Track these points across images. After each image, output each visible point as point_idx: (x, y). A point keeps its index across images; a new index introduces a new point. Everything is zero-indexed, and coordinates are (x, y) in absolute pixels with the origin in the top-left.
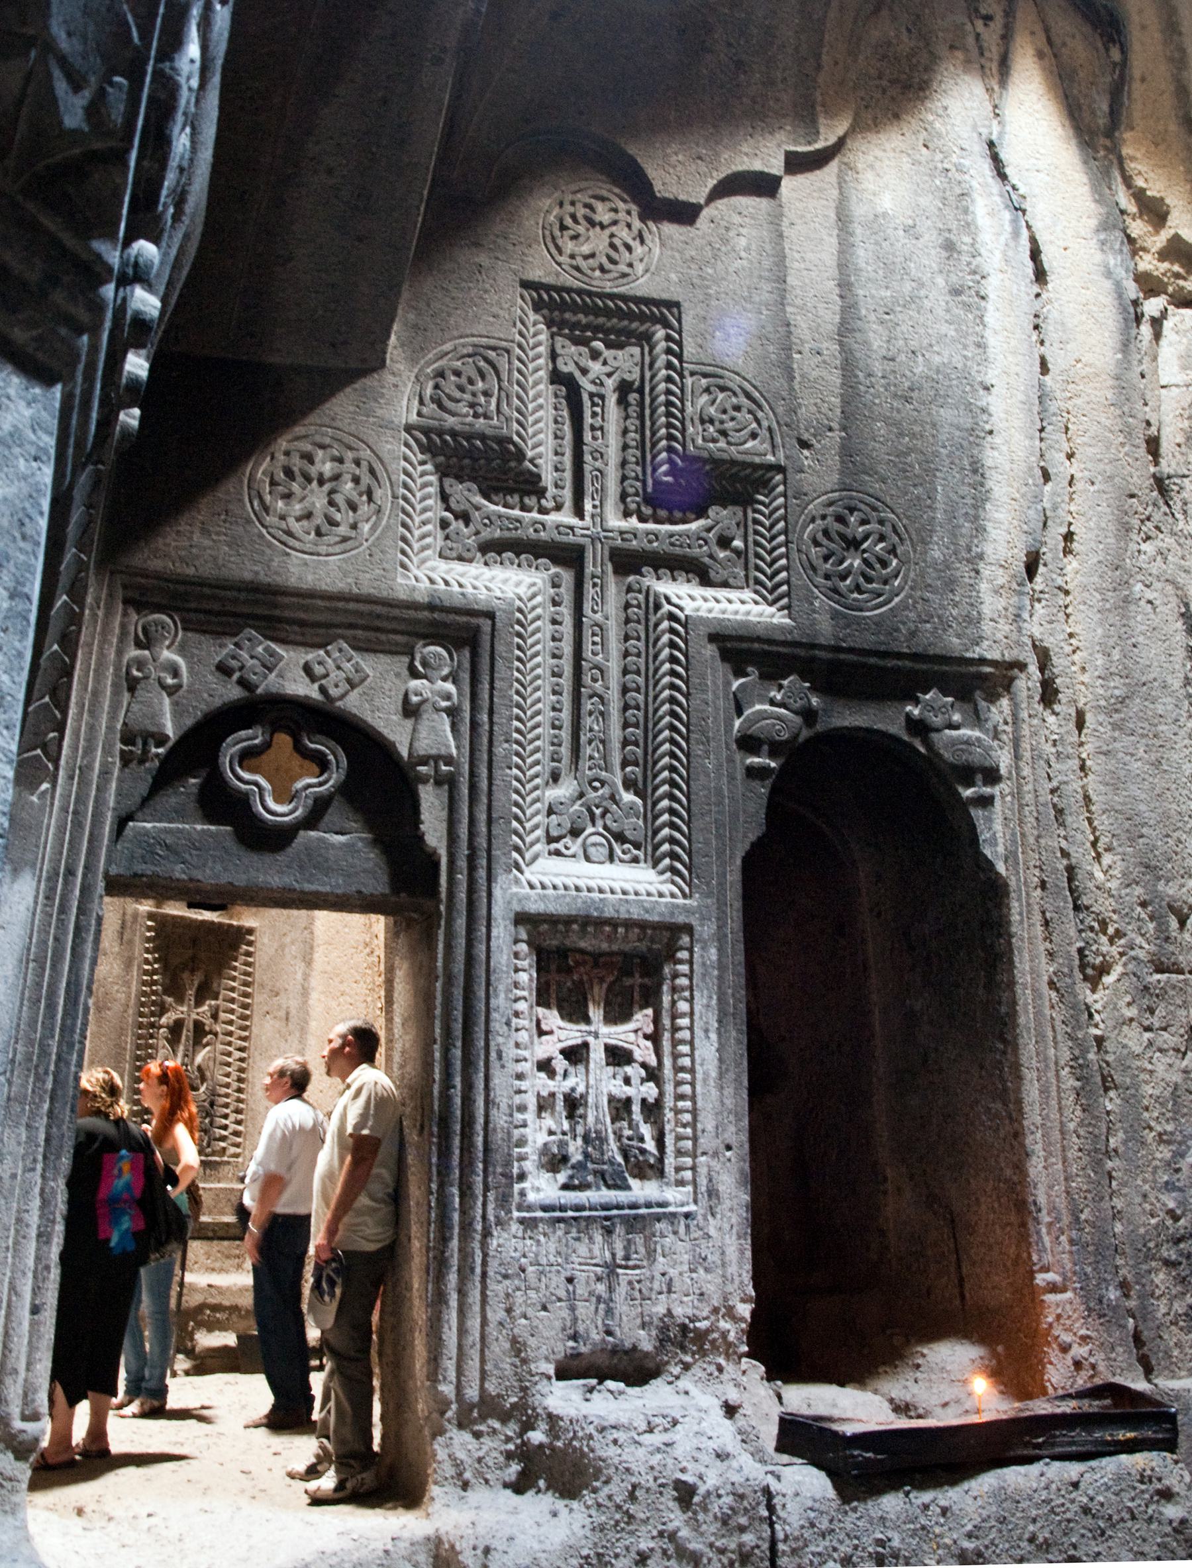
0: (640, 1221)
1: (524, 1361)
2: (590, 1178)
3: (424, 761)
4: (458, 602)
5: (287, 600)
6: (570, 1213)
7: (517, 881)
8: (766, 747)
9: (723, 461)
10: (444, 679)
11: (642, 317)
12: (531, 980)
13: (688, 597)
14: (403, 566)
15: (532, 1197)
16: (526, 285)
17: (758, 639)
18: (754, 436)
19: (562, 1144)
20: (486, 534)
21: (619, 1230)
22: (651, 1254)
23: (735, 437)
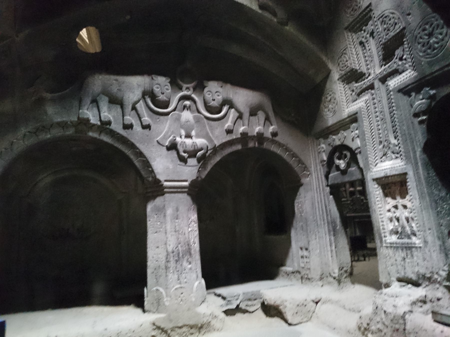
0: (409, 248)
1: (390, 277)
2: (403, 237)
3: (356, 149)
4: (352, 114)
5: (334, 126)
6: (395, 245)
7: (372, 171)
8: (421, 114)
9: (391, 39)
10: (357, 130)
11: (367, 14)
12: (380, 193)
13: (394, 83)
14: (344, 110)
15: (388, 241)
16: (346, 29)
17: (409, 85)
18: (396, 24)
19: (397, 229)
20: (357, 93)
21: (404, 250)
22: (412, 256)
23: (392, 28)
